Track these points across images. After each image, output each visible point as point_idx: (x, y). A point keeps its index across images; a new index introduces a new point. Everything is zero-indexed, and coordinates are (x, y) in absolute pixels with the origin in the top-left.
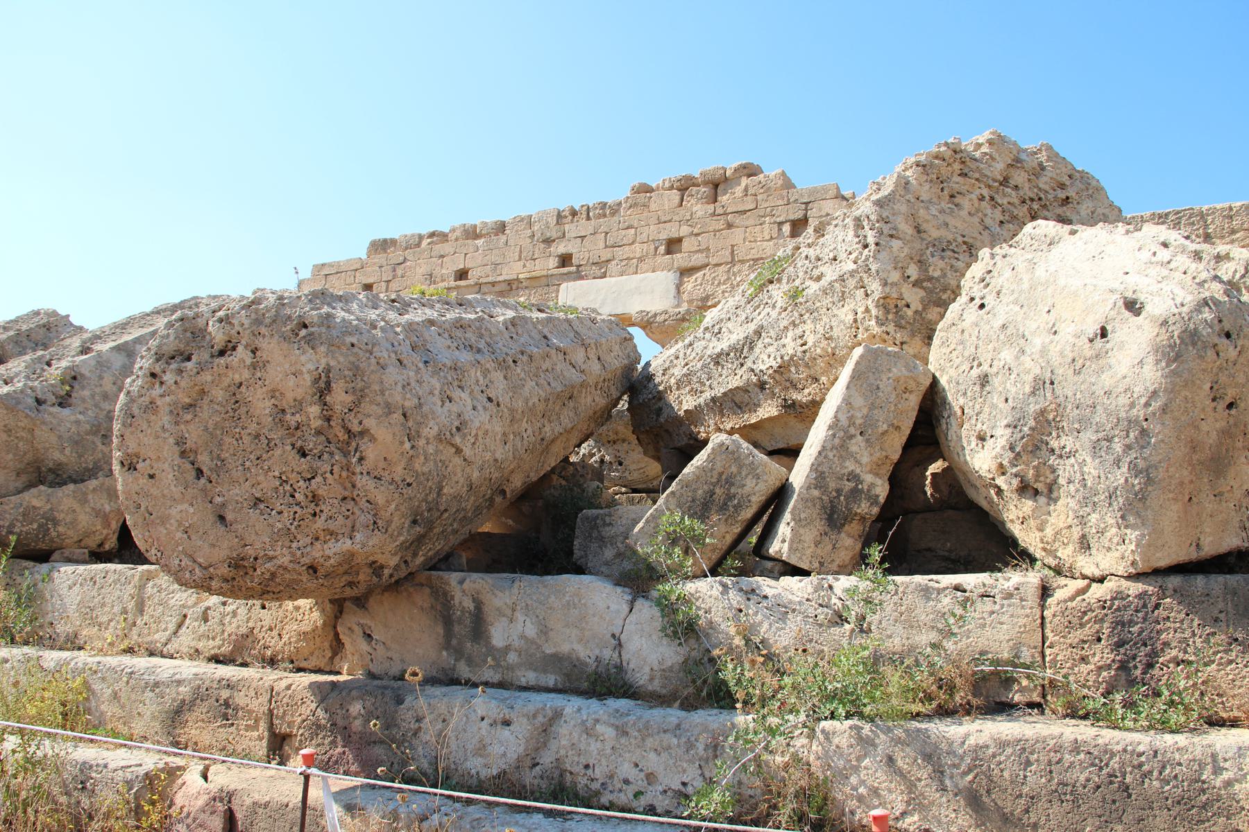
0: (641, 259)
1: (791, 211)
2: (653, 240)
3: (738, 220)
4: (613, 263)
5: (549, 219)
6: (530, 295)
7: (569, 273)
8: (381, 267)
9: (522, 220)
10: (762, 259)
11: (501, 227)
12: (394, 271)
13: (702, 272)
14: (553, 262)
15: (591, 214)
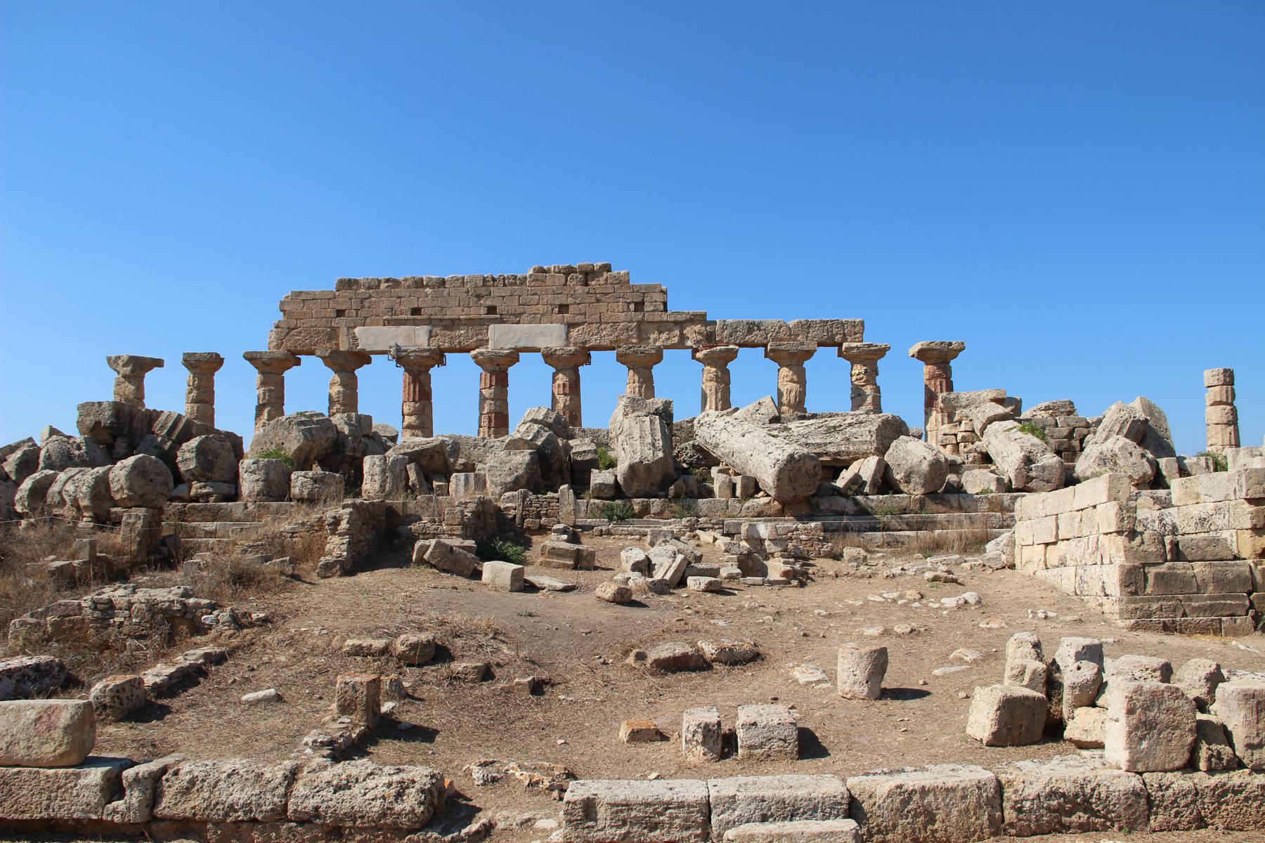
0: (543, 315)
7: (496, 318)
8: (351, 299)
9: (458, 279)
11: (442, 283)
12: (362, 303)
14: (483, 310)
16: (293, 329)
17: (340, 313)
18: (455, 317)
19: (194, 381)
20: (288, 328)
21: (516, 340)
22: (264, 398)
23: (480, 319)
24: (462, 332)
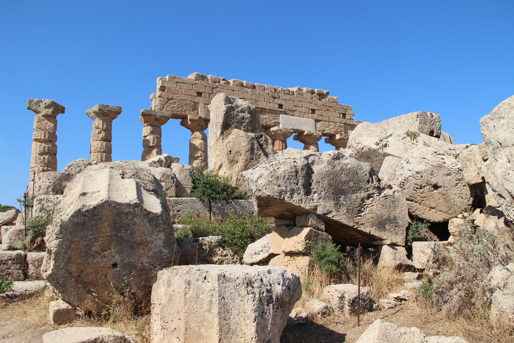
1: (342, 111)
2: (308, 108)
3: (330, 109)
4: (296, 112)
5: (272, 89)
6: (270, 116)
8: (205, 87)
9: (262, 86)
10: (336, 122)
12: (212, 90)
13: (322, 122)
14: (277, 106)
15: (285, 92)
16: (170, 100)
17: (200, 94)
18: (264, 107)
19: (103, 125)
20: (168, 98)
21: (293, 125)
22: (153, 143)
23: (276, 110)
24: (267, 116)
